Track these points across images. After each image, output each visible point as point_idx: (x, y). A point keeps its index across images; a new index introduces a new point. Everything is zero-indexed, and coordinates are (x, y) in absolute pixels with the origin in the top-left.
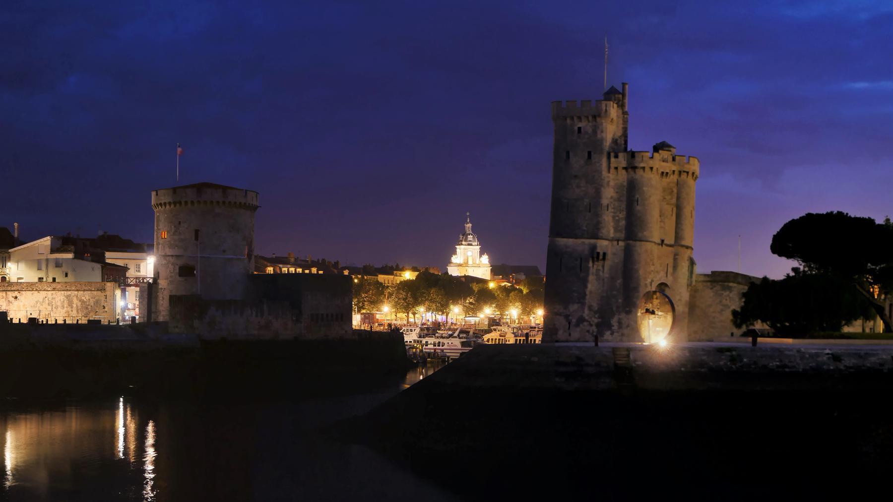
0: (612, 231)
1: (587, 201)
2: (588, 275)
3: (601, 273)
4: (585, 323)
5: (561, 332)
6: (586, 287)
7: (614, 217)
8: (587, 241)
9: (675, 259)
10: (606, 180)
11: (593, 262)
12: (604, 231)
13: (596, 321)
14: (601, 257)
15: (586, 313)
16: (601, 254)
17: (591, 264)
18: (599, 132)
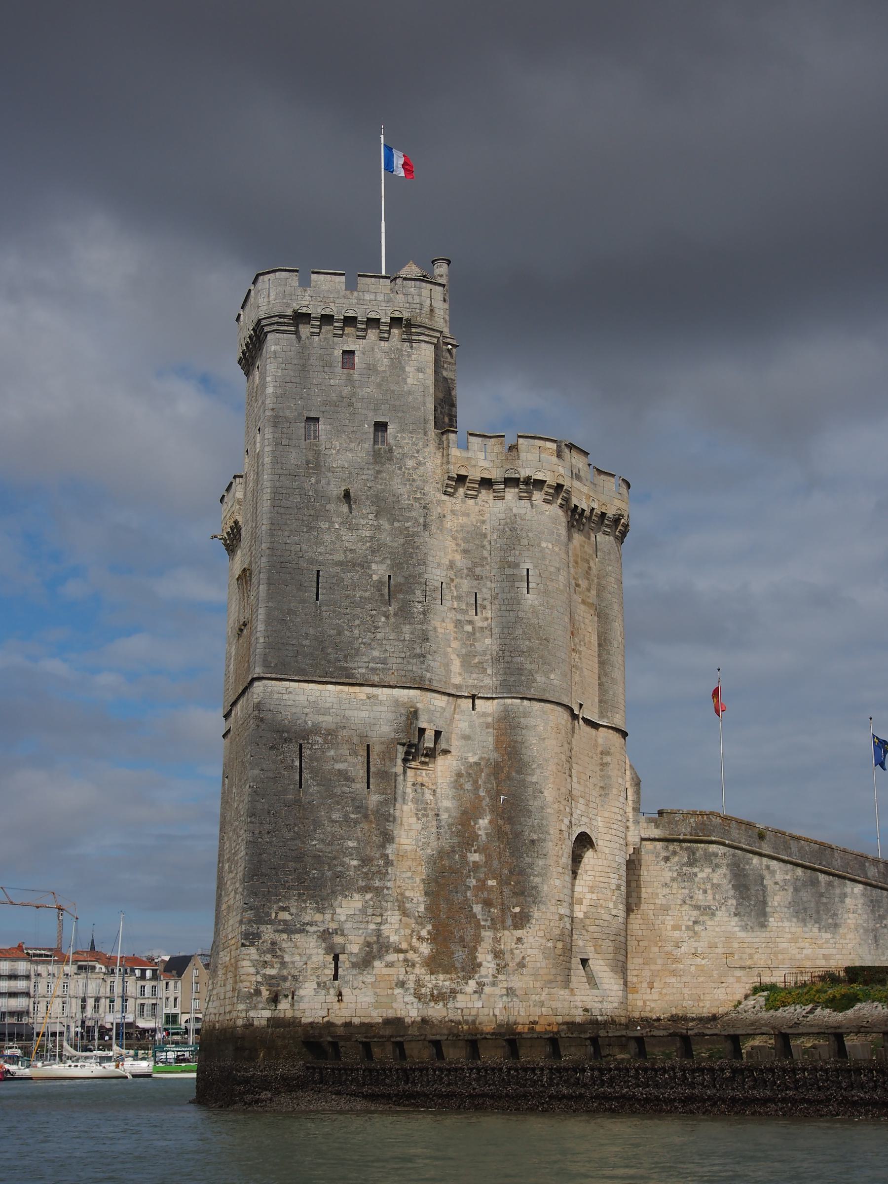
0: (456, 665)
1: (379, 570)
2: (391, 799)
3: (428, 796)
4: (392, 957)
5: (307, 990)
6: (388, 838)
7: (458, 624)
8: (384, 693)
9: (603, 765)
10: (436, 511)
11: (405, 760)
12: (435, 663)
13: (425, 949)
14: (428, 742)
15: (394, 929)
16: (429, 735)
17: (399, 769)
18: (408, 369)
